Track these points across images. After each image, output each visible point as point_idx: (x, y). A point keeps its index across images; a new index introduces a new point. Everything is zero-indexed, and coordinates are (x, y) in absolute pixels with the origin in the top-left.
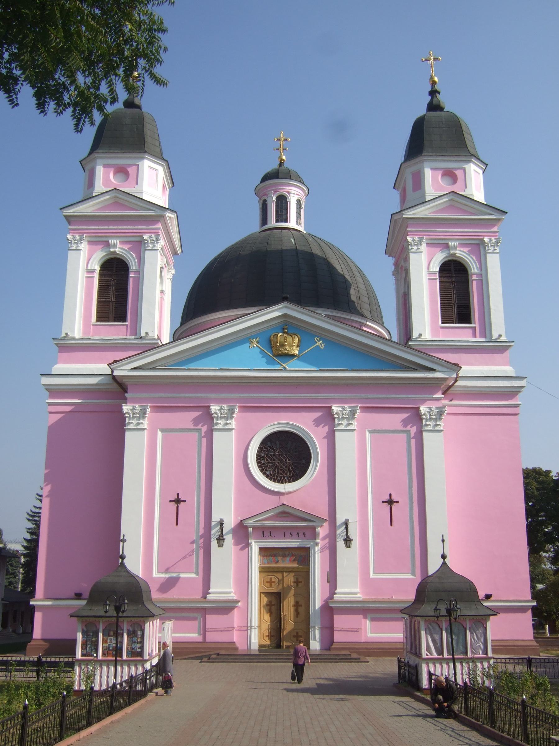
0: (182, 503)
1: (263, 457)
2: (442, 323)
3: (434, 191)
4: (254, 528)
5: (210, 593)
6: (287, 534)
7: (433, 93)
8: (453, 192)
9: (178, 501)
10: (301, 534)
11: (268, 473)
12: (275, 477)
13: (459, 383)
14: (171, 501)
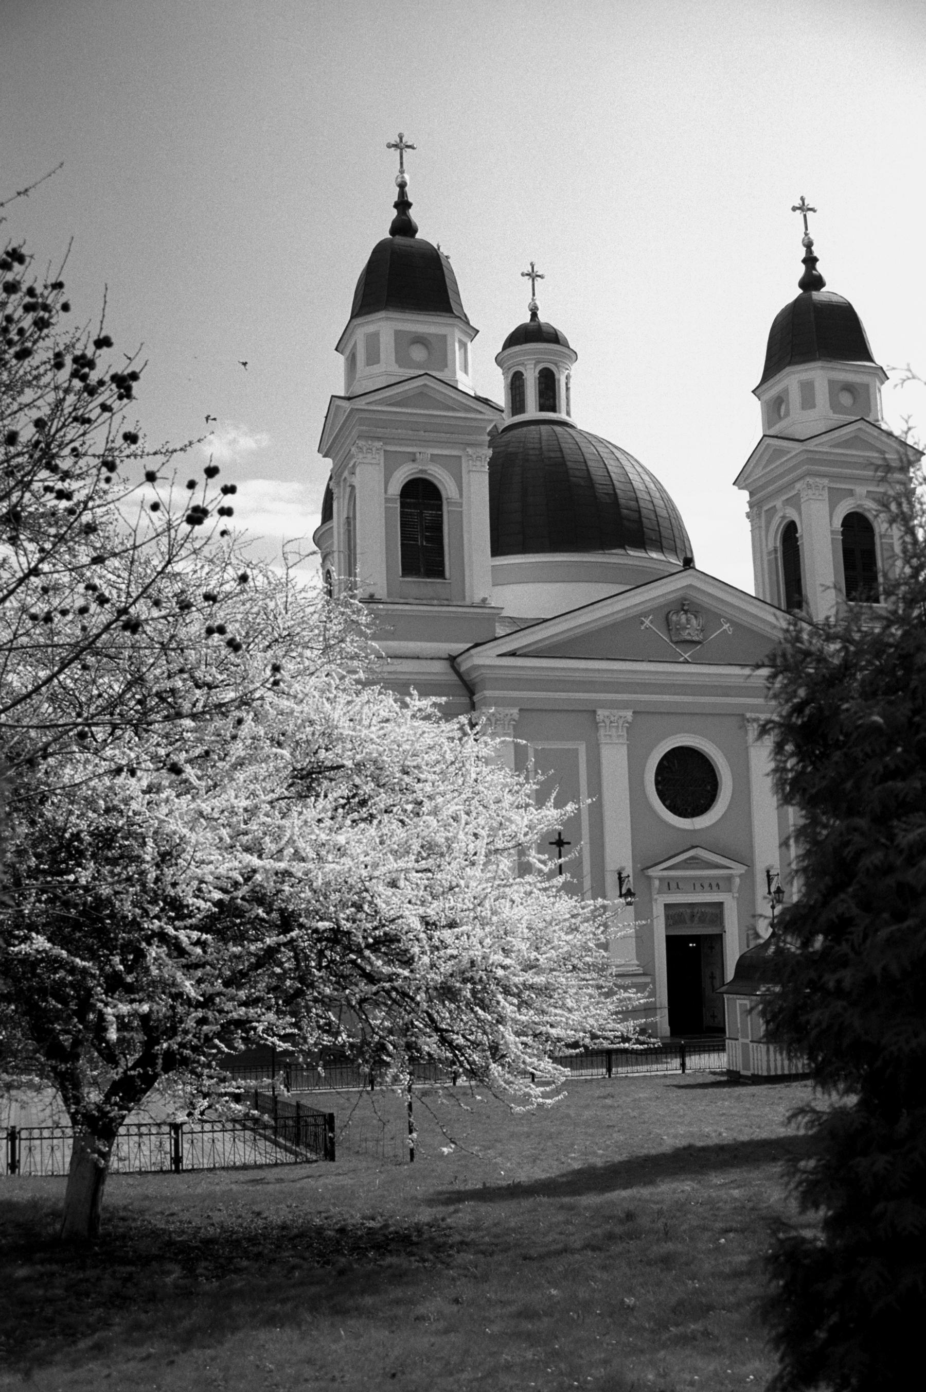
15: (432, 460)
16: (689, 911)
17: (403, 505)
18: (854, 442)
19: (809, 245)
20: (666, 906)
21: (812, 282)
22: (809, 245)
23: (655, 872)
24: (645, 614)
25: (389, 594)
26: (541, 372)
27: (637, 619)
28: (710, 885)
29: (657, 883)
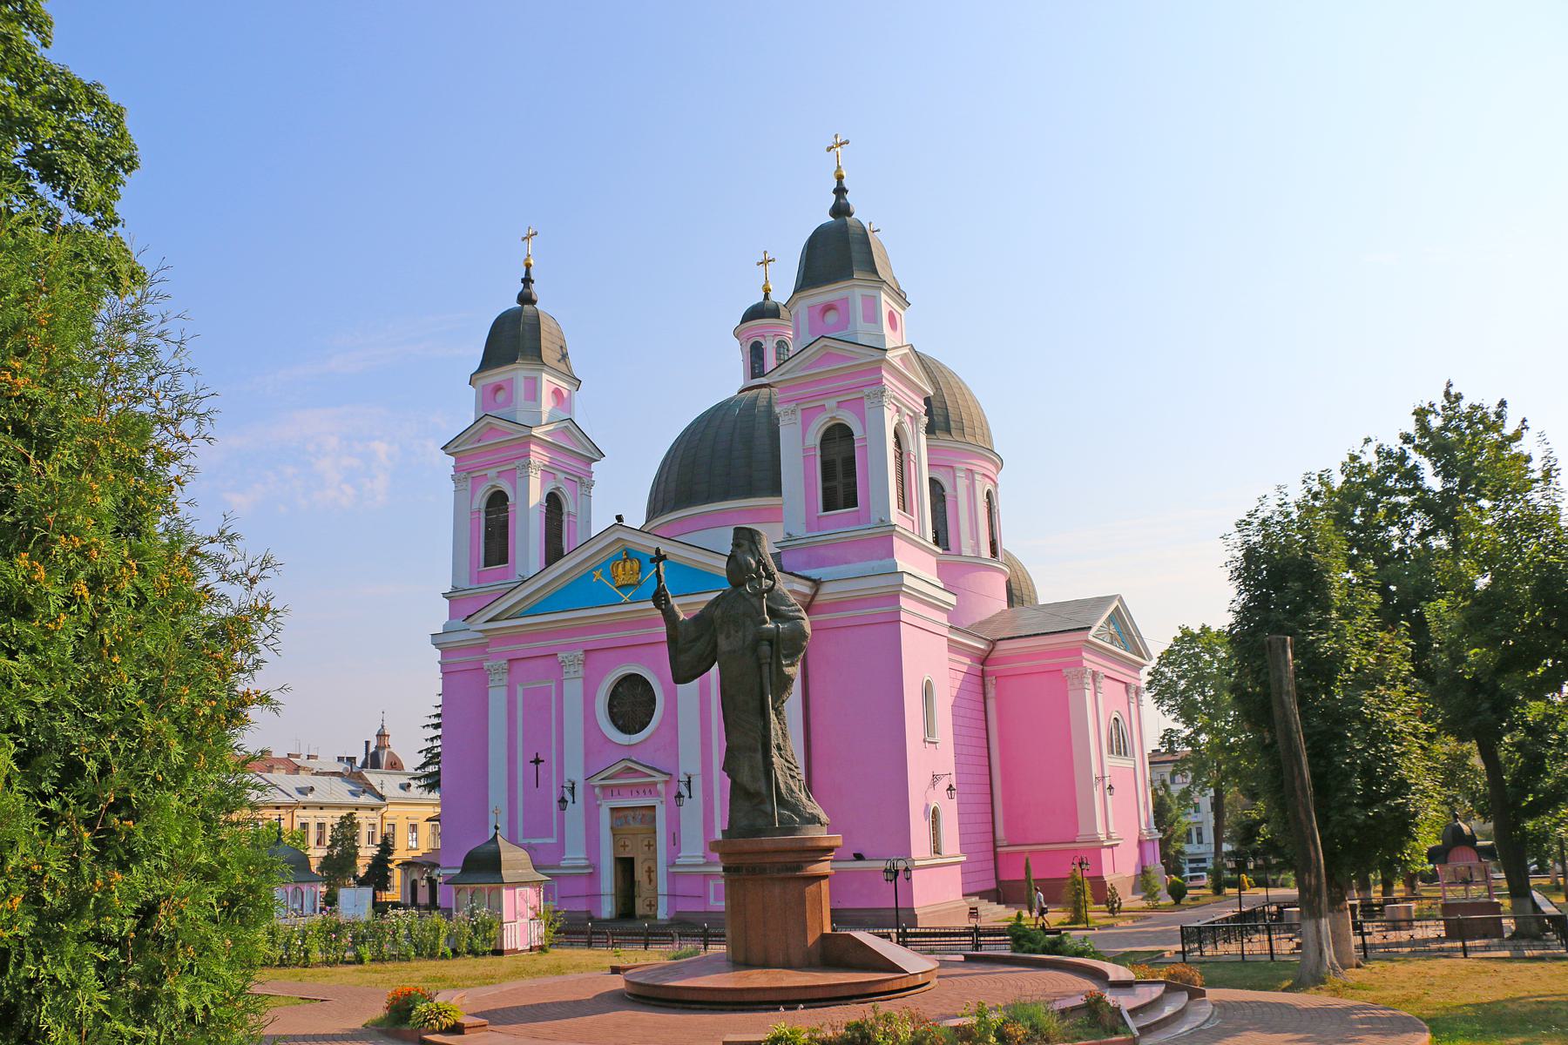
0: (541, 763)
1: (615, 706)
2: (826, 510)
3: (813, 337)
4: (603, 788)
5: (564, 860)
6: (635, 793)
7: (840, 191)
8: (823, 336)
9: (537, 761)
10: (641, 792)
11: (620, 722)
12: (626, 729)
13: (826, 589)
14: (531, 762)
15: (498, 477)
16: (632, 814)
17: (487, 513)
18: (828, 357)
19: (840, 178)
20: (612, 809)
21: (841, 210)
22: (840, 178)
23: (596, 781)
24: (596, 569)
25: (471, 583)
26: (752, 346)
27: (589, 575)
28: (644, 791)
29: (597, 790)
